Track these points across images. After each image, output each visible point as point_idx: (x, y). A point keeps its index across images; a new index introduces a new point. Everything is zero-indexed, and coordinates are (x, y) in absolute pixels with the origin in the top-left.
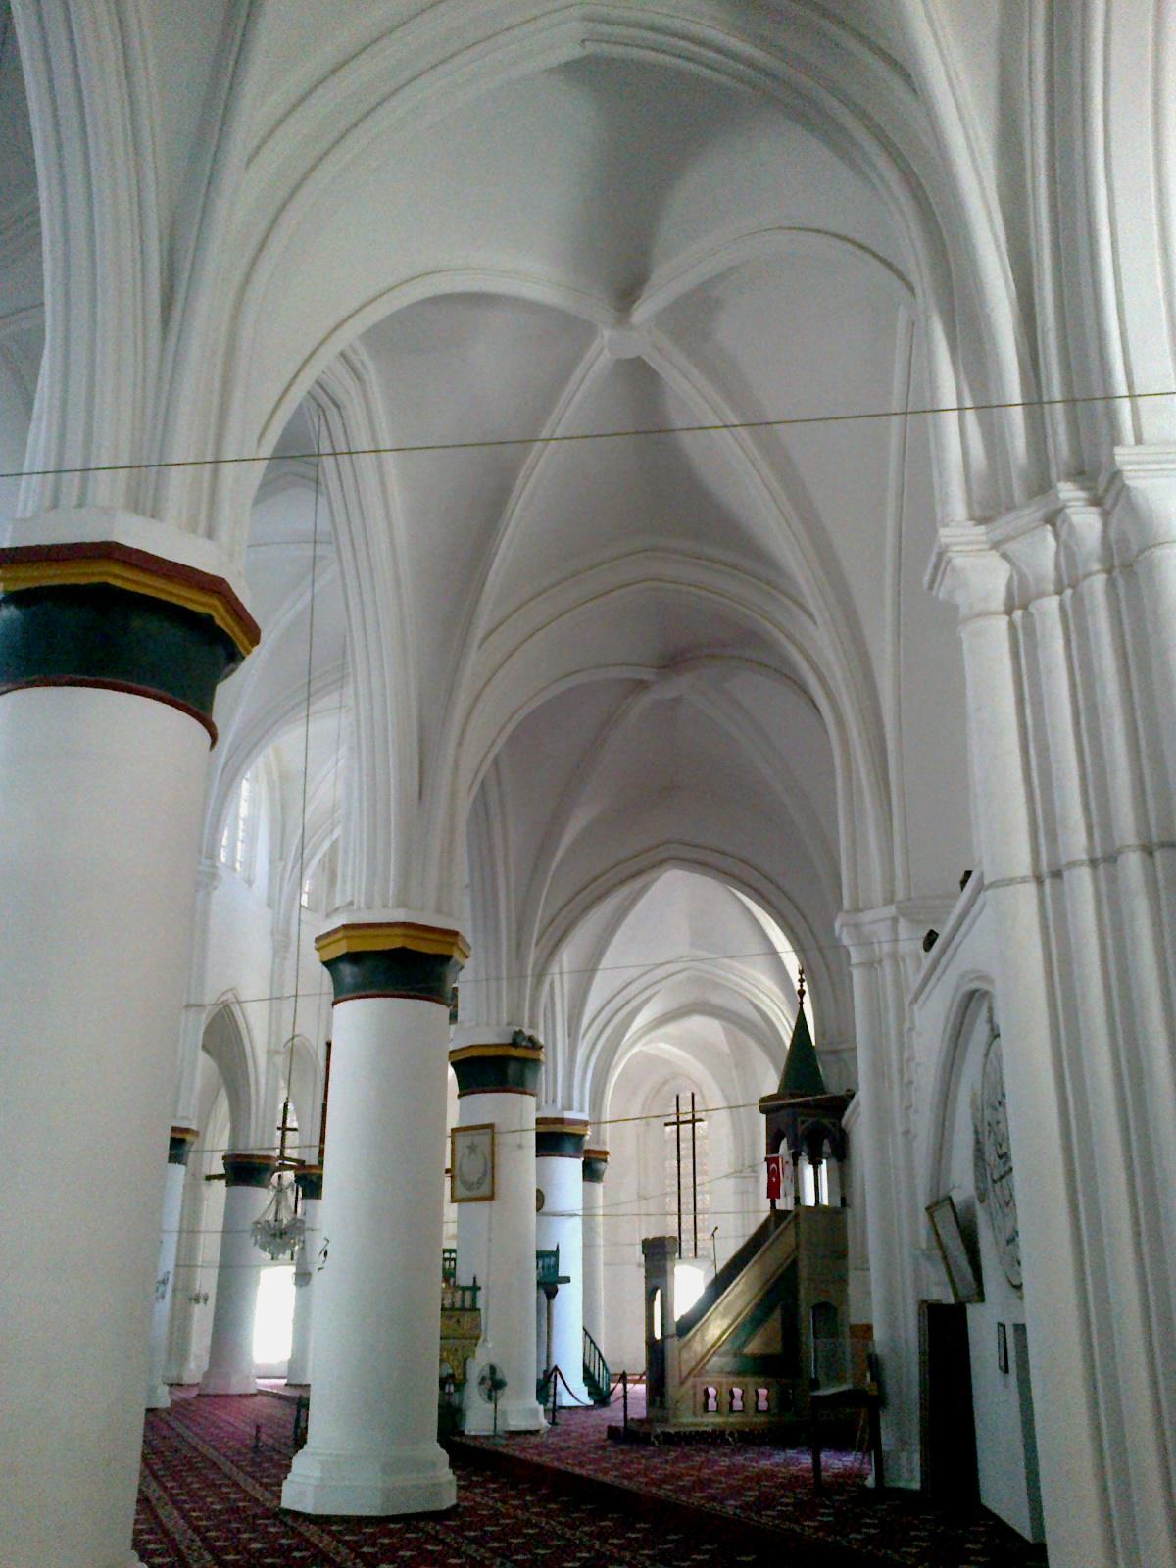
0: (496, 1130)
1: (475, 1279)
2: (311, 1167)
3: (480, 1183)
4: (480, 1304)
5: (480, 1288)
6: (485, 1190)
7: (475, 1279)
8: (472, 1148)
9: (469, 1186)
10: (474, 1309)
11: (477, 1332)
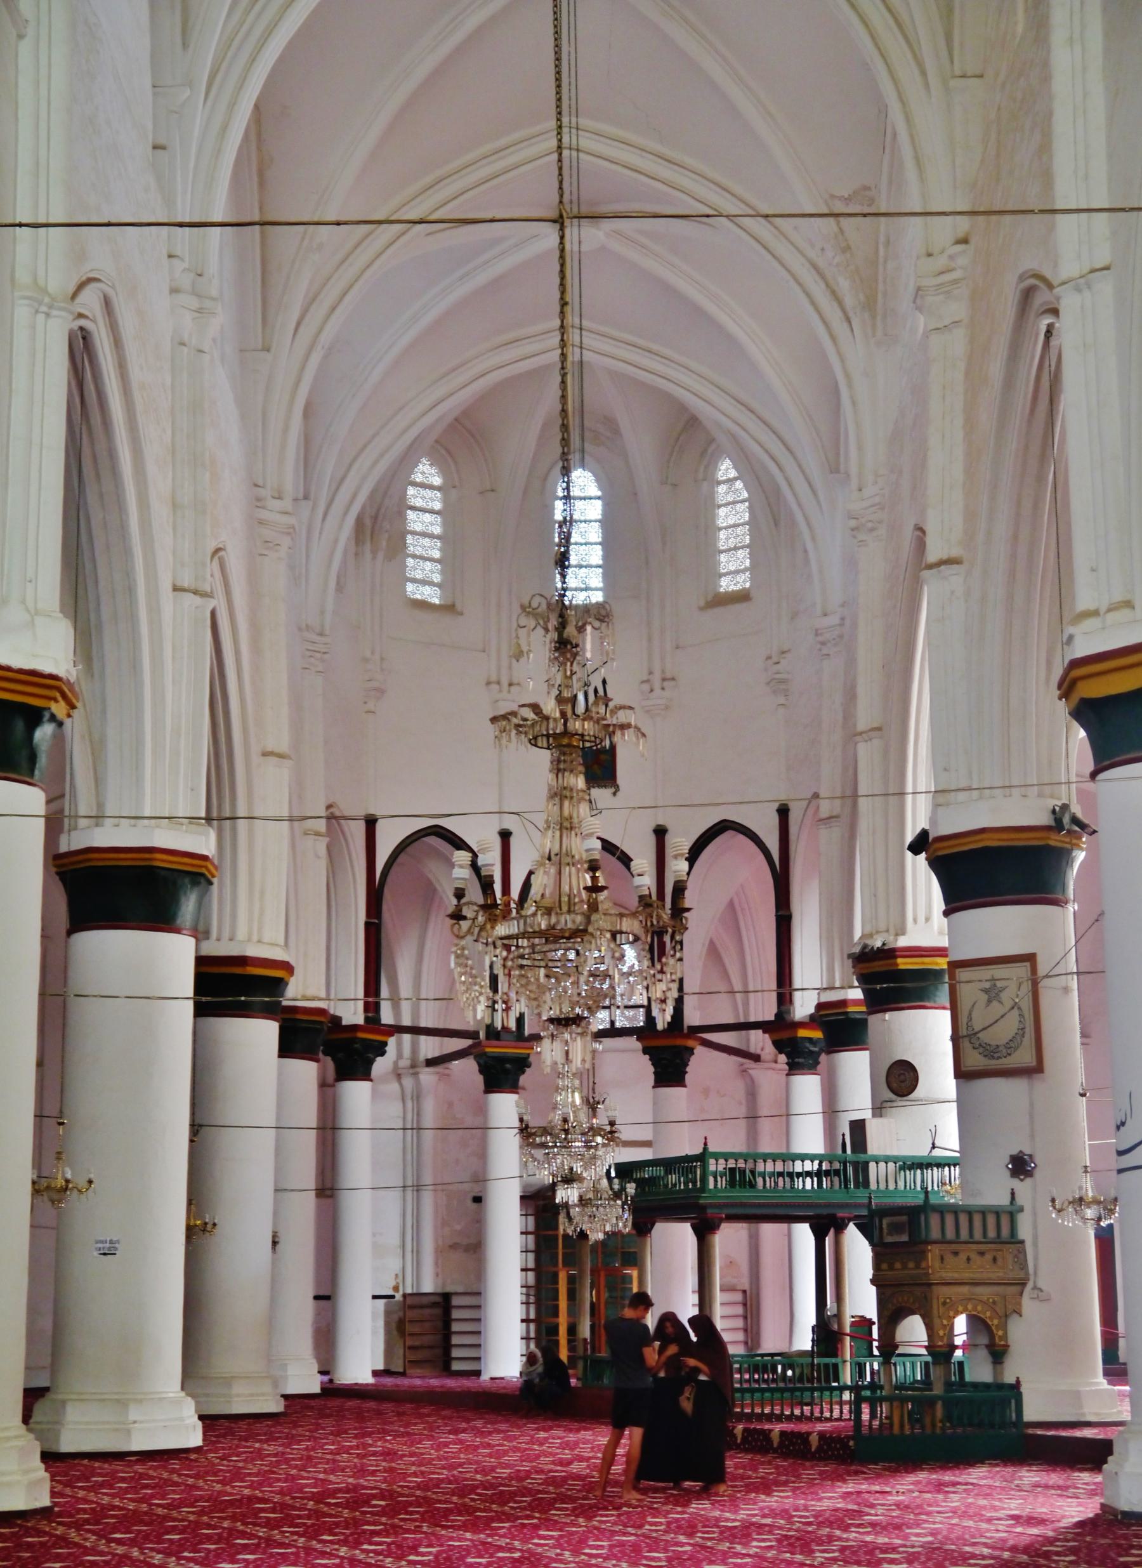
0: (1042, 970)
1: (1013, 1194)
2: (354, 1028)
3: (1011, 1046)
4: (1024, 1231)
5: (1021, 1209)
6: (1024, 1056)
7: (1013, 1194)
8: (992, 993)
9: (990, 1052)
10: (1015, 1241)
11: (1022, 1275)
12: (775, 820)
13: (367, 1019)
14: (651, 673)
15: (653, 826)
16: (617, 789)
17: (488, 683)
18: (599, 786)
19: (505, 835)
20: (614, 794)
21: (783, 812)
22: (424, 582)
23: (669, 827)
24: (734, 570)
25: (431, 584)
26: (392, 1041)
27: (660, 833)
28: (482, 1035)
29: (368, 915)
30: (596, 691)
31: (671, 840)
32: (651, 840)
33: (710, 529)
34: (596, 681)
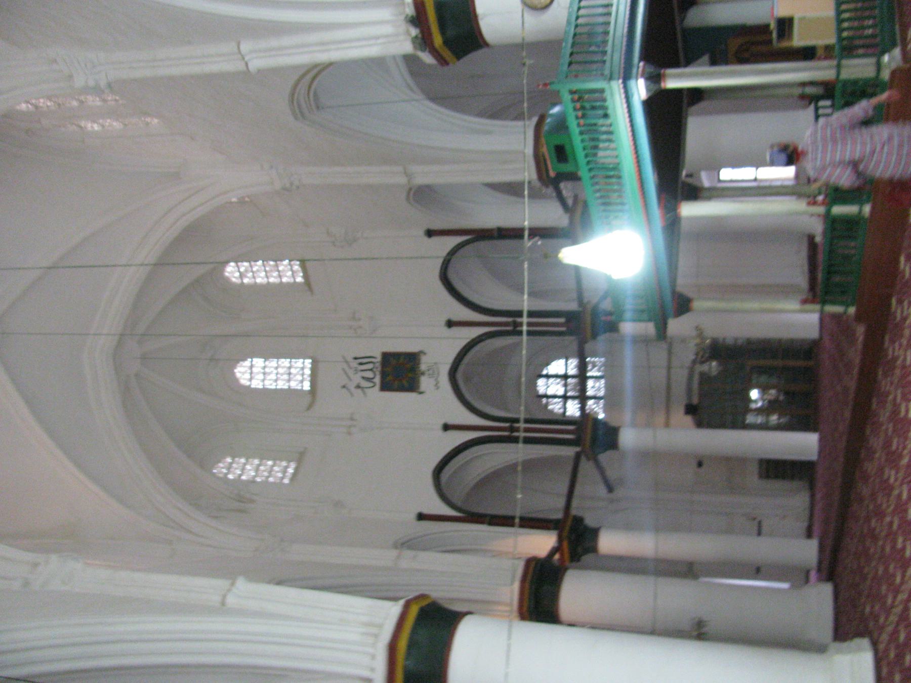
12: (436, 240)
13: (555, 528)
14: (351, 327)
15: (446, 328)
16: (421, 352)
17: (349, 433)
18: (419, 364)
19: (447, 427)
20: (425, 354)
21: (430, 233)
22: (284, 472)
23: (446, 319)
24: (288, 272)
25: (287, 467)
26: (574, 512)
27: (450, 324)
28: (578, 449)
29: (482, 523)
30: (361, 364)
31: (455, 318)
32: (456, 330)
33: (267, 288)
34: (354, 364)
